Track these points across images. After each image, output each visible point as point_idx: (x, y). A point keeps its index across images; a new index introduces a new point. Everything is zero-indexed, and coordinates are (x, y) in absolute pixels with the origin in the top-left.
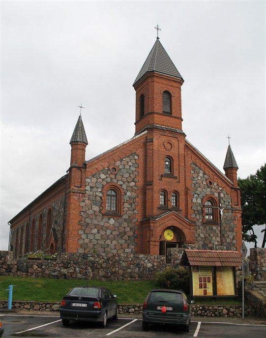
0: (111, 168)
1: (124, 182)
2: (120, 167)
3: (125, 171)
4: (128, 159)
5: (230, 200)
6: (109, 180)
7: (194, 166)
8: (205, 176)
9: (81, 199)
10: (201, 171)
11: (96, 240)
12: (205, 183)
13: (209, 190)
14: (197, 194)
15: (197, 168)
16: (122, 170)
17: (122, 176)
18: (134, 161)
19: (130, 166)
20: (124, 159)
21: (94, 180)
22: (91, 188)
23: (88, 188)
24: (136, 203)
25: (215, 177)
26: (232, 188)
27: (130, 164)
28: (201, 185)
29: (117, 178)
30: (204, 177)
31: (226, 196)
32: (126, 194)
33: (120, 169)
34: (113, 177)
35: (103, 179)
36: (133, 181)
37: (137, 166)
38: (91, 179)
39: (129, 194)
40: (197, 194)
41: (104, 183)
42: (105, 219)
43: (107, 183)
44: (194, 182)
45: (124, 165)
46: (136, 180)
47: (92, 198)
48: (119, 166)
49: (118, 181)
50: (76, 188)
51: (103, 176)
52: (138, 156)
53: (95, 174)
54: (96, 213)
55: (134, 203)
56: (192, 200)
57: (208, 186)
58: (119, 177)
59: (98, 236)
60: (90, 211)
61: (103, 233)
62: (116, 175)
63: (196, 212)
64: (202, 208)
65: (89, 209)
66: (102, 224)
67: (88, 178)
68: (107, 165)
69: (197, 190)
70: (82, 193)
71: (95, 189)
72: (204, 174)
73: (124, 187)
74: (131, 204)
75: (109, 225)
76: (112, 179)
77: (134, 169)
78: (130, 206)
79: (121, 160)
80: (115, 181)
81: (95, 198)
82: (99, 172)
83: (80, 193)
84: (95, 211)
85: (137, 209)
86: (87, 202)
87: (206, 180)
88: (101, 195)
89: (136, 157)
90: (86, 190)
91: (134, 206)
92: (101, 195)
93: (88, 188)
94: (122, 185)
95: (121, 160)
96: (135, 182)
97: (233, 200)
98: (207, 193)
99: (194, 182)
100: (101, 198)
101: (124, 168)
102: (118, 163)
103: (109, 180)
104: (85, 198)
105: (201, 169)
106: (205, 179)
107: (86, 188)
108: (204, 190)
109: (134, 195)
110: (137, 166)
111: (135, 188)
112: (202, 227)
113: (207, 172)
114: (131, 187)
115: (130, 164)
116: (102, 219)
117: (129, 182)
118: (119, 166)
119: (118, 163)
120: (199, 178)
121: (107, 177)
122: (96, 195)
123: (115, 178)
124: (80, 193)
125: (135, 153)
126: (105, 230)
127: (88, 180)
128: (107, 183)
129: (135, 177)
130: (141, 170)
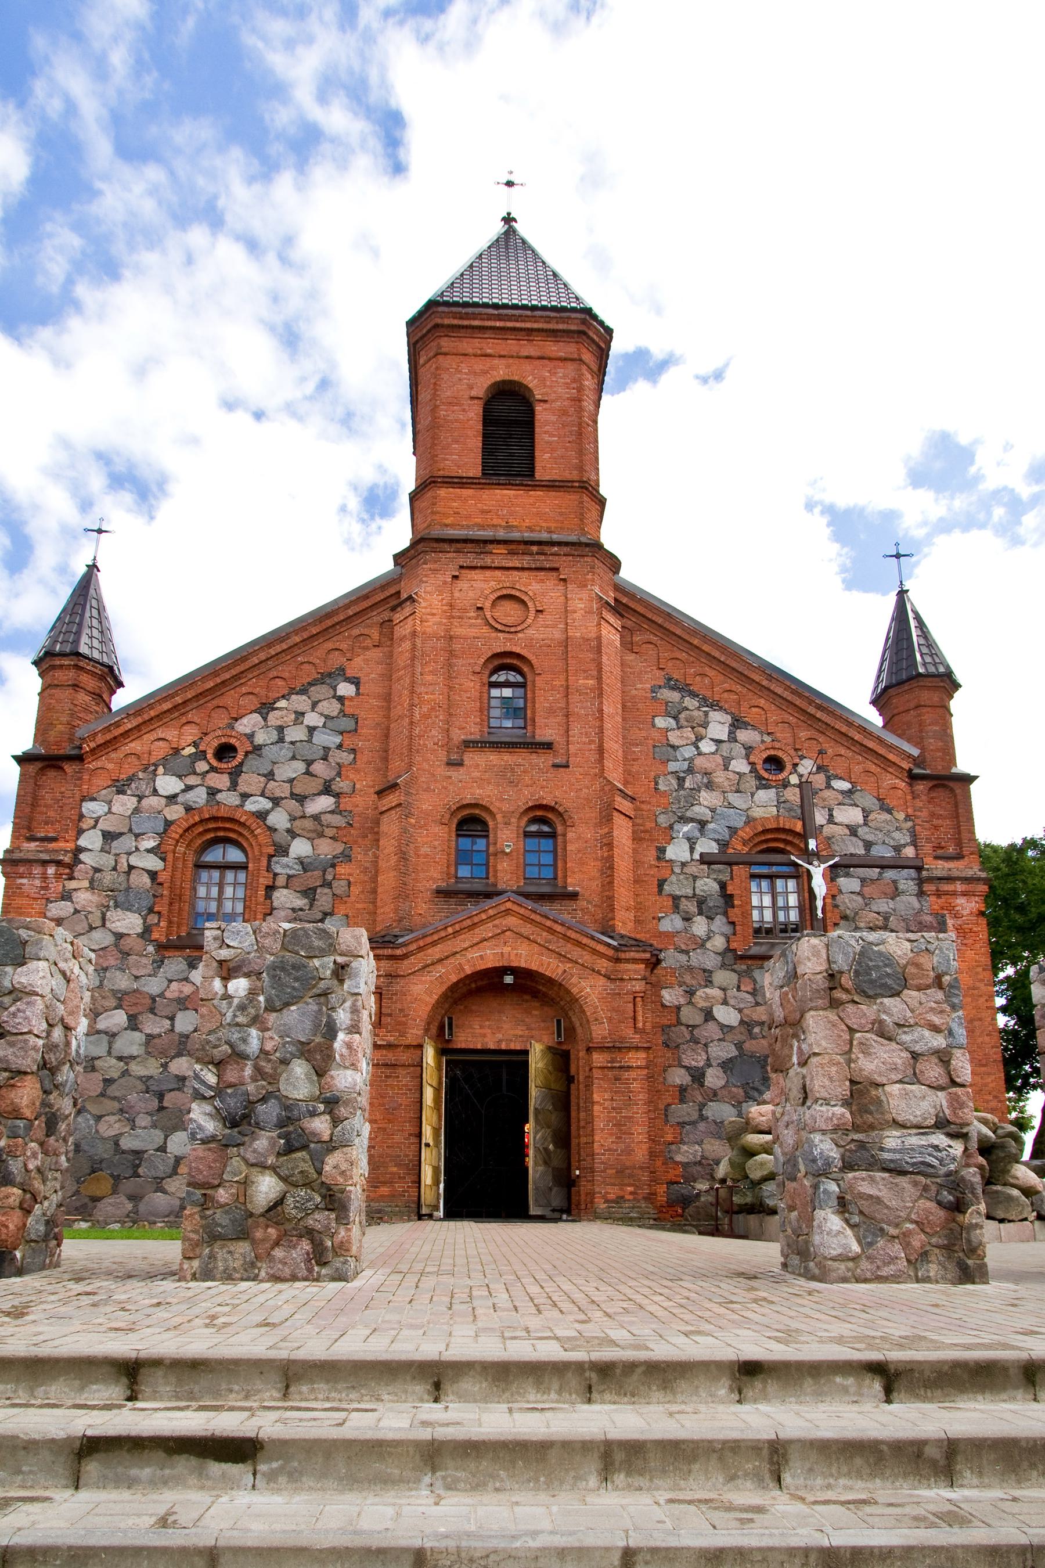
0: (210, 746)
1: (276, 801)
2: (260, 738)
3: (286, 752)
4: (300, 702)
5: (903, 838)
6: (199, 797)
7: (675, 696)
8: (743, 735)
9: (56, 888)
10: (715, 716)
11: (120, 1059)
12: (740, 765)
13: (763, 795)
14: (692, 820)
15: (690, 702)
16: (270, 752)
17: (270, 776)
18: (332, 707)
19: (311, 730)
20: (282, 704)
21: (124, 804)
22: (109, 837)
23: (91, 840)
24: (339, 887)
25: (803, 734)
26: (913, 778)
27: (312, 719)
28: (720, 777)
29: (242, 787)
30: (732, 738)
31: (880, 817)
32: (283, 850)
33: (257, 749)
34: (221, 781)
35: (172, 799)
36: (327, 790)
37: (347, 724)
38: (109, 803)
39: (300, 848)
40: (692, 820)
41: (175, 812)
42: (175, 965)
43: (188, 809)
44: (672, 766)
45: (281, 729)
46: (341, 785)
47: (108, 878)
48: (251, 736)
49: (245, 796)
50: (33, 845)
51: (168, 784)
52: (356, 682)
53: (131, 779)
54: (126, 944)
55: (329, 885)
56: (662, 850)
57: (759, 778)
58: (250, 781)
59: (131, 1043)
60: (96, 935)
61: (154, 1025)
62: (235, 774)
63: (692, 907)
64: (723, 886)
65: (91, 928)
66: (153, 986)
67: (94, 799)
68: (191, 733)
69: (692, 799)
70: (59, 863)
71: (127, 842)
72: (737, 724)
73: (279, 819)
74: (309, 893)
75: (188, 989)
76: (212, 792)
77: (323, 738)
78: (300, 902)
79: (265, 708)
80: (228, 799)
81: (122, 878)
82: (151, 770)
83: (45, 863)
84: (119, 936)
85: (342, 909)
86: (84, 898)
87: (749, 749)
88: (153, 863)
89: (345, 689)
90: (79, 850)
91: (324, 900)
92: (153, 863)
93: (91, 840)
94: (267, 812)
95: (265, 708)
96: (337, 795)
97: (923, 833)
98: (757, 813)
99: (672, 766)
100: (153, 875)
101: (281, 740)
102: (249, 723)
103: (199, 797)
104: (72, 885)
105: (716, 706)
106: (738, 749)
107: (82, 842)
108: (734, 798)
109: (327, 849)
110: (347, 724)
111: (337, 820)
112: (724, 977)
113: (752, 715)
114: (316, 818)
115: (312, 719)
116: (159, 963)
117: (301, 799)
118: (251, 736)
119: (249, 723)
120: (706, 746)
121: (189, 788)
122: (131, 868)
123: (234, 786)
124: (45, 863)
125: (342, 671)
126: (167, 1012)
127: (92, 808)
128: (188, 809)
129: (339, 774)
130: (367, 742)
